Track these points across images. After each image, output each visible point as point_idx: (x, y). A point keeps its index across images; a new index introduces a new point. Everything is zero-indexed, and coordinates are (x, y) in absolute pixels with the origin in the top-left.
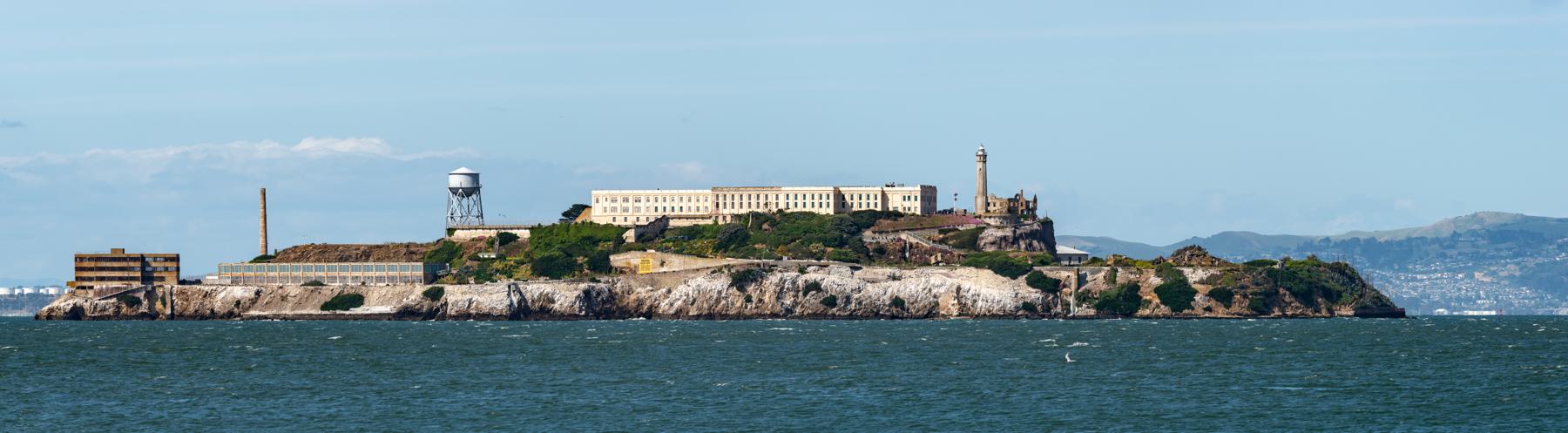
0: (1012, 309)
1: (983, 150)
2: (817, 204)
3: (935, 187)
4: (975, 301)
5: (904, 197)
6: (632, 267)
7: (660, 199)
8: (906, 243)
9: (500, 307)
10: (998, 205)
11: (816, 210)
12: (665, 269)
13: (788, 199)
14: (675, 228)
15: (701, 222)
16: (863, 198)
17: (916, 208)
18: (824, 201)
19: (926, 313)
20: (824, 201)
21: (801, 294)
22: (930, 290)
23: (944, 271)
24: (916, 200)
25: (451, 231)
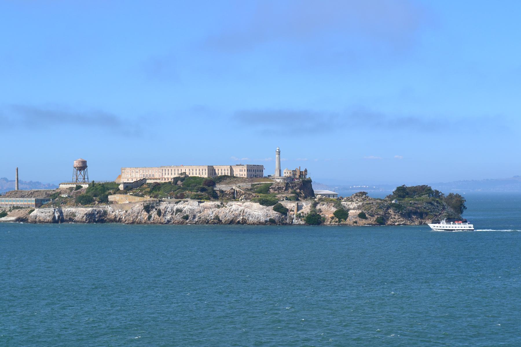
0: (264, 222)
1: (279, 149)
2: (201, 173)
5: (240, 170)
6: (117, 201)
8: (234, 191)
9: (48, 218)
10: (289, 173)
11: (200, 176)
14: (148, 183)
15: (158, 181)
16: (222, 171)
17: (245, 175)
19: (229, 223)
21: (174, 213)
22: (232, 212)
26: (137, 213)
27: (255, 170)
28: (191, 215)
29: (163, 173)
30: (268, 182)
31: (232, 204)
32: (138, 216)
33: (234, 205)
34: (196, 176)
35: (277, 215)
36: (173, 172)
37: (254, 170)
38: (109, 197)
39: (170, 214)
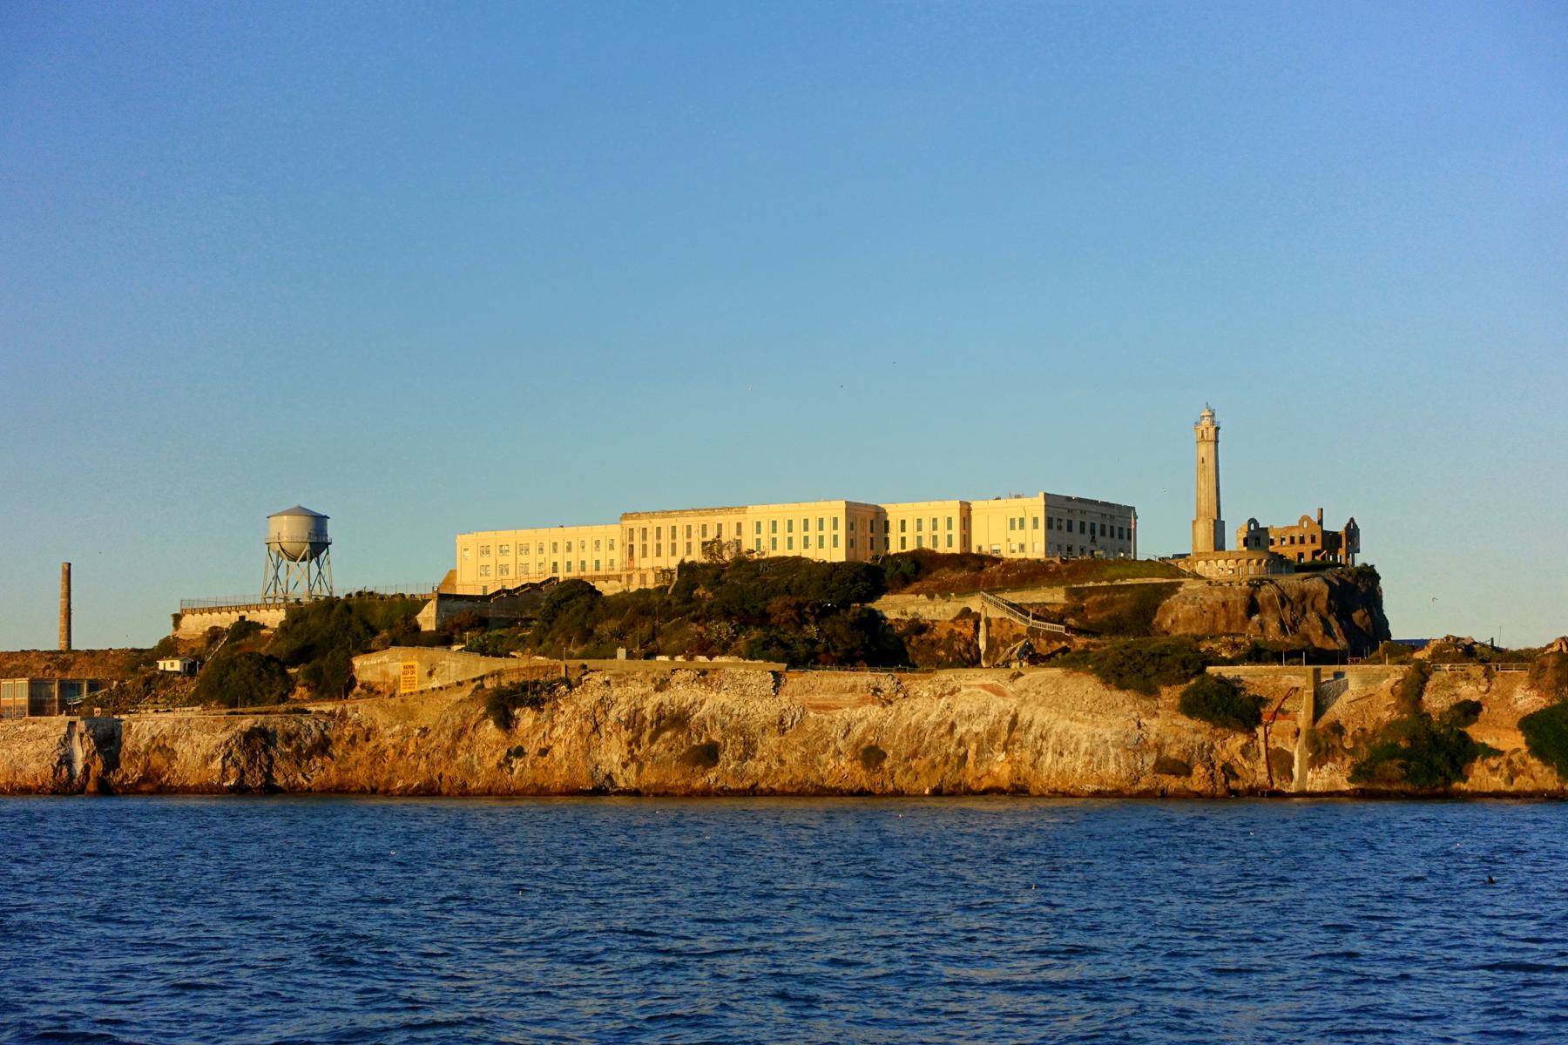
2: (813, 541)
3: (1127, 512)
4: (1040, 753)
5: (1012, 521)
7: (561, 547)
9: (33, 767)
11: (806, 554)
12: (436, 684)
13: (759, 531)
18: (828, 532)
20: (828, 532)
21: (645, 738)
22: (953, 726)
23: (989, 681)
24: (1036, 526)
25: (177, 619)
26: (453, 734)
27: (1093, 525)
28: (729, 741)
29: (632, 546)
30: (1157, 580)
31: (955, 683)
32: (454, 750)
33: (964, 690)
34: (790, 554)
35: (1198, 737)
36: (681, 541)
37: (1088, 528)
38: (358, 662)
39: (626, 735)
